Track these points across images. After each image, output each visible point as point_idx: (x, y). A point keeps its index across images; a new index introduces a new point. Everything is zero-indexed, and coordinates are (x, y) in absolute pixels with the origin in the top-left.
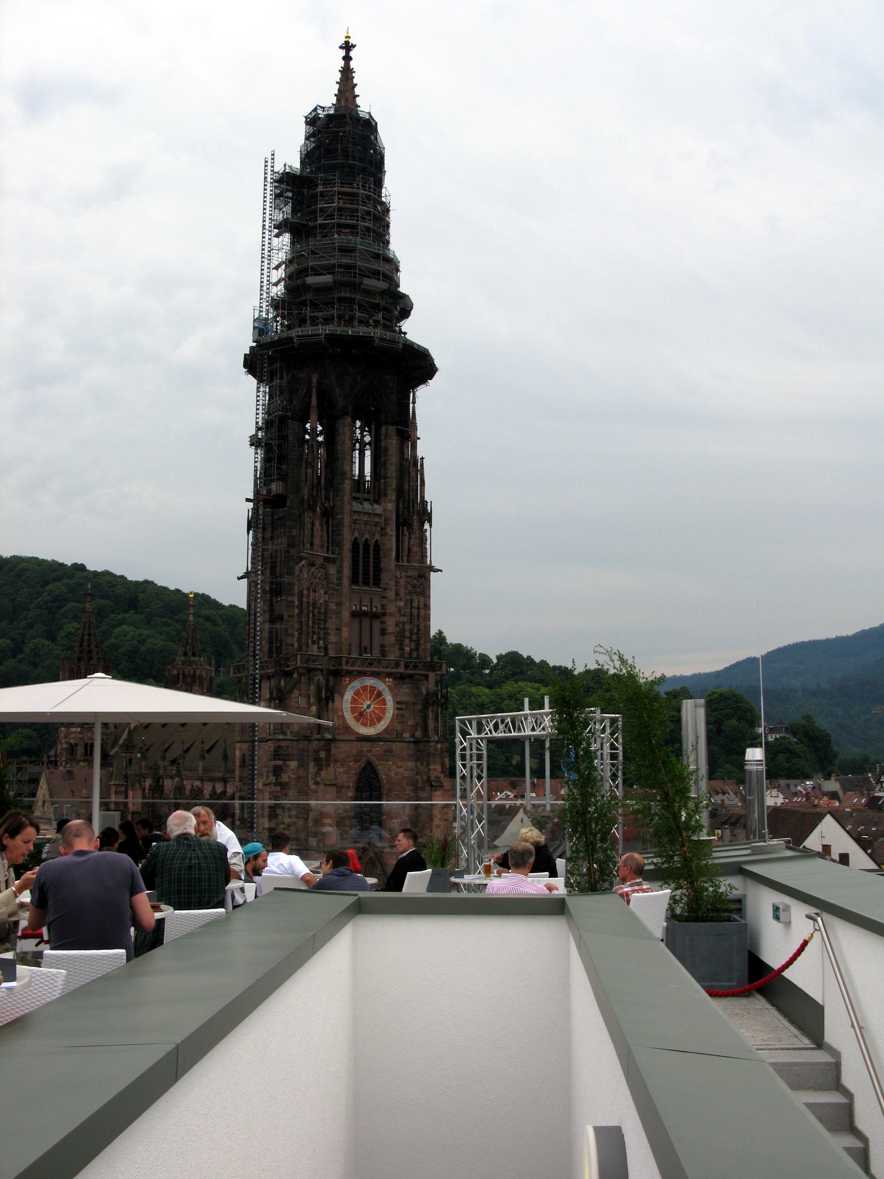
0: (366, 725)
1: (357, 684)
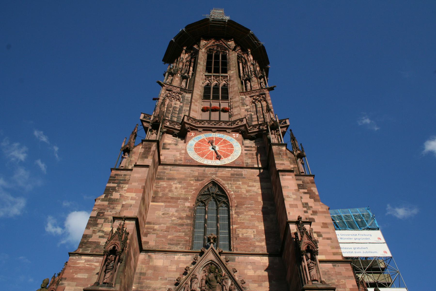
0: (211, 159)
1: (204, 136)
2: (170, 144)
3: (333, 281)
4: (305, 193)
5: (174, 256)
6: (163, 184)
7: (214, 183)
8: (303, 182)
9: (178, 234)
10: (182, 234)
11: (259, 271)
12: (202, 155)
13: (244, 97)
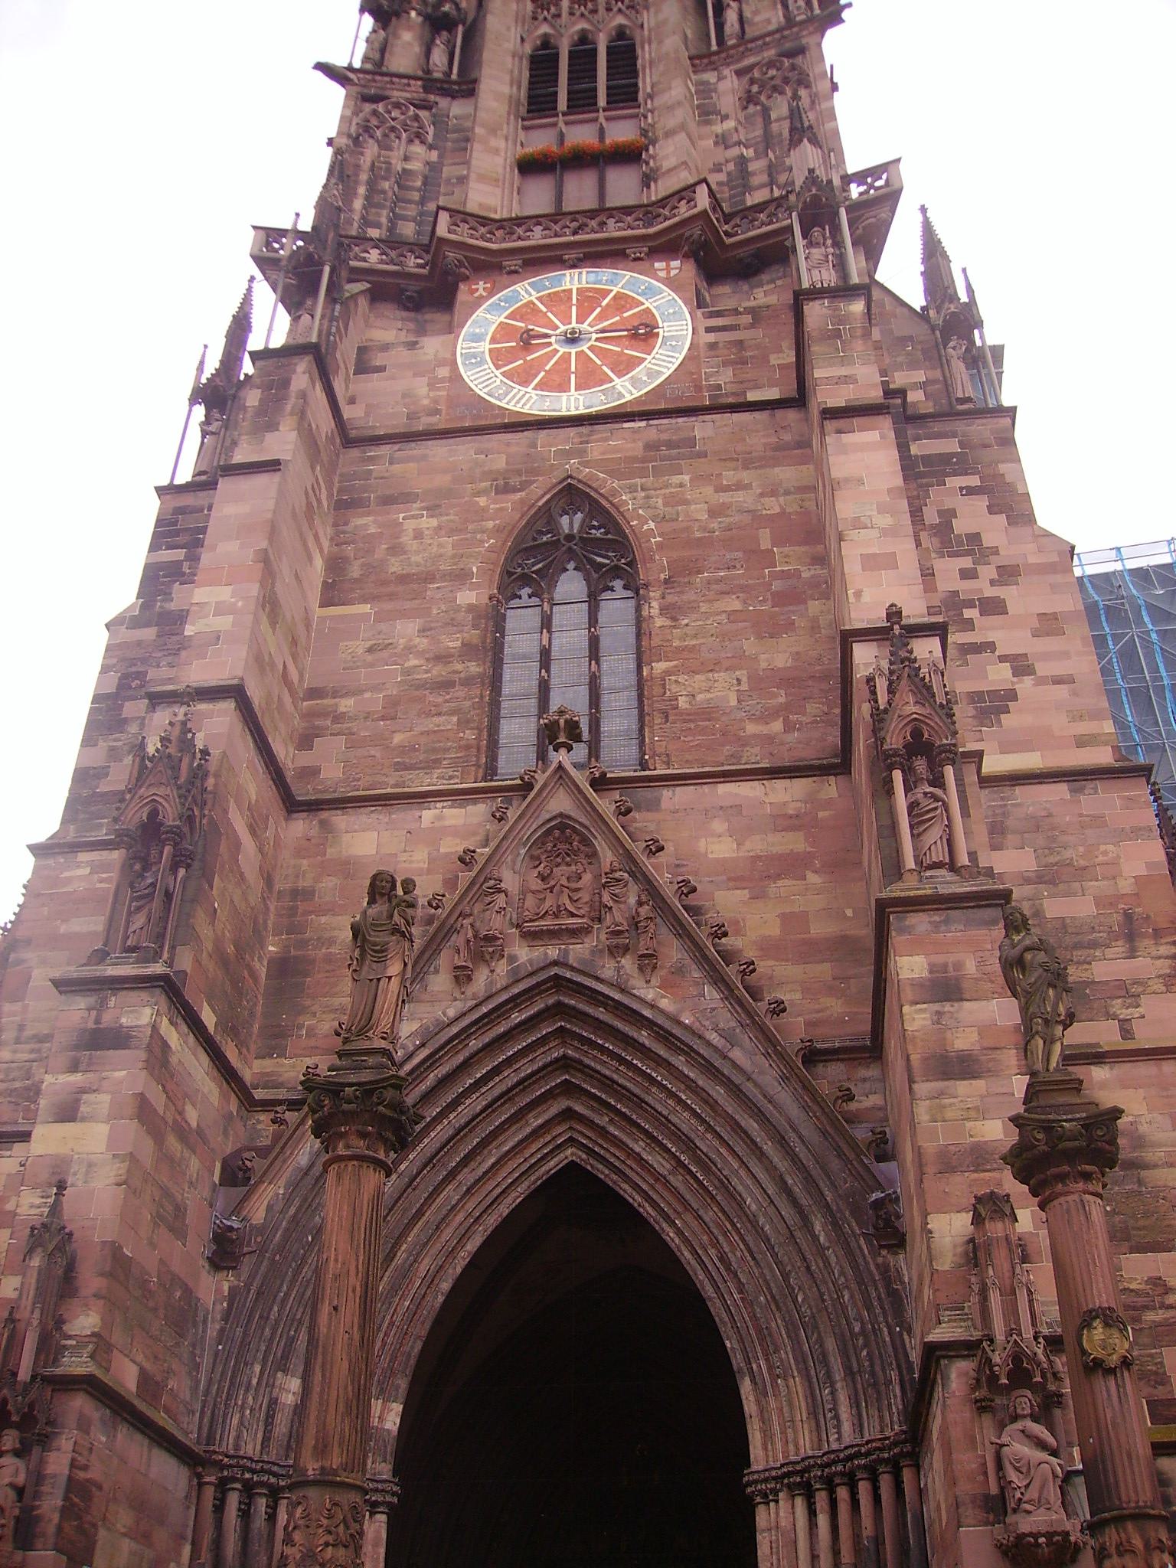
1: (526, 291)
2: (385, 347)
3: (1068, 854)
4: (970, 491)
5: (417, 813)
6: (365, 522)
7: (573, 494)
8: (961, 444)
9: (431, 724)
10: (447, 724)
11: (758, 837)
12: (523, 377)
13: (710, 77)
